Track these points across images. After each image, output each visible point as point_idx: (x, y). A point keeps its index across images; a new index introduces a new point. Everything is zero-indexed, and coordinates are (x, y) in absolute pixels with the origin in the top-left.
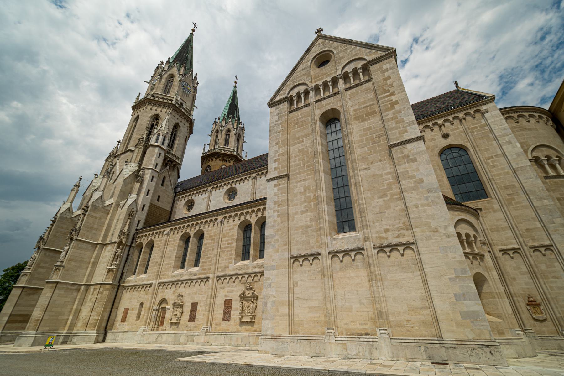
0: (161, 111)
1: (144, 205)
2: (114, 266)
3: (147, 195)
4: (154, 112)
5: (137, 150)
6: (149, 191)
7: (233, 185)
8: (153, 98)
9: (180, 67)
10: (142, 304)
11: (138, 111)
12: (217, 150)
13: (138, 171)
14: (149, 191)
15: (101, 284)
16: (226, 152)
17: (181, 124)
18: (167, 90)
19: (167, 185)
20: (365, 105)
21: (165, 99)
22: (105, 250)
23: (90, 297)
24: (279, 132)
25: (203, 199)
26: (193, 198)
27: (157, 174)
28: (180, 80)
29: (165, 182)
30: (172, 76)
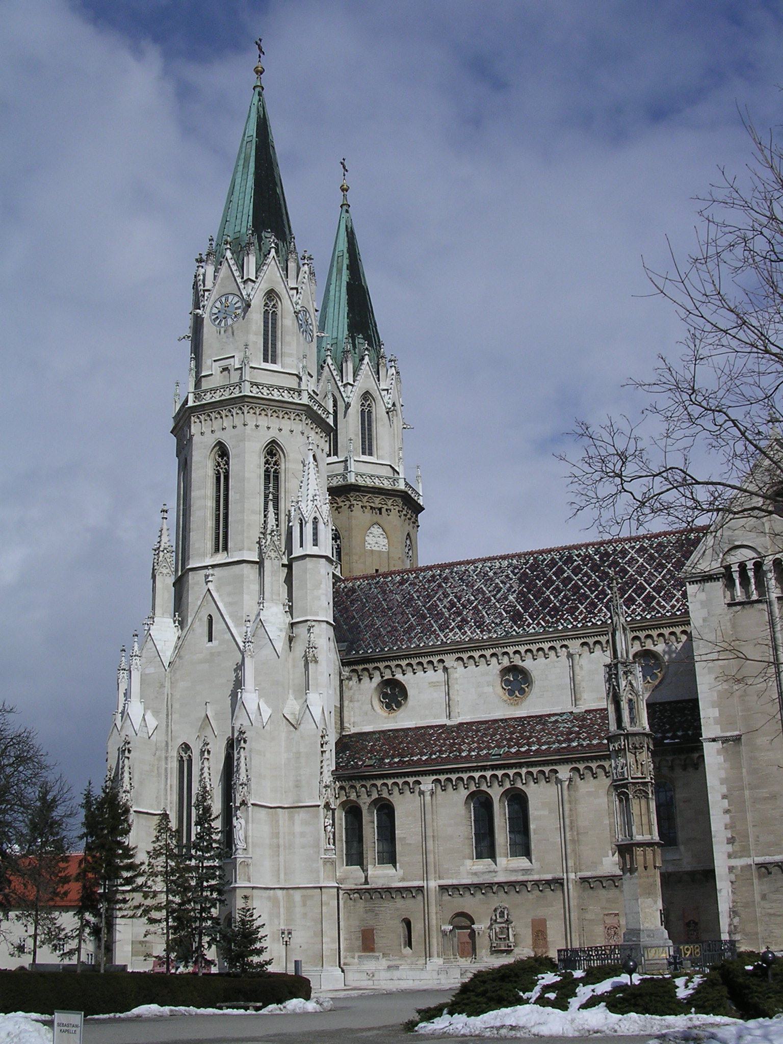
2: (330, 853)
7: (517, 661)
8: (255, 392)
9: (277, 252)
10: (408, 923)
11: (217, 424)
12: (352, 479)
13: (292, 625)
15: (321, 888)
16: (377, 483)
18: (270, 354)
21: (279, 388)
22: (291, 818)
23: (299, 910)
25: (433, 685)
26: (399, 676)
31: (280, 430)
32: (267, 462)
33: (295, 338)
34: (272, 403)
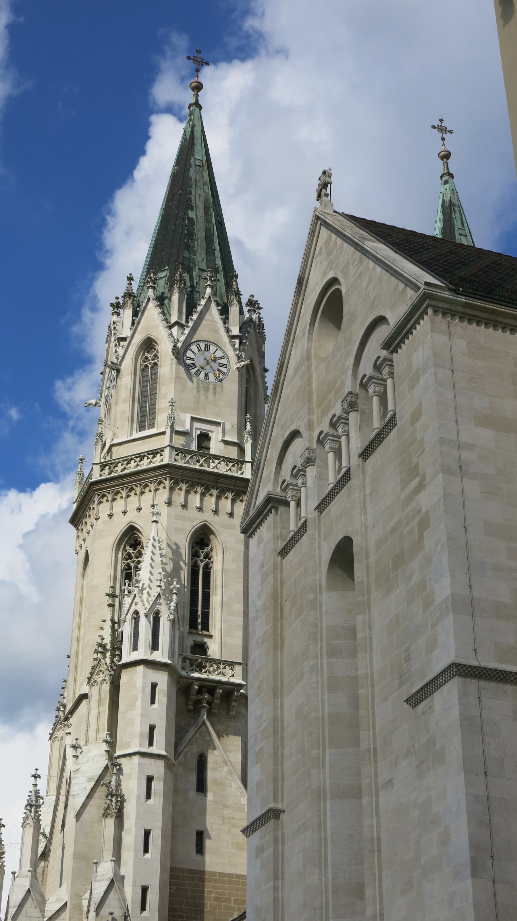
0: (139, 509)
1: (145, 890)
3: (146, 850)
4: (120, 525)
5: (96, 689)
6: (147, 833)
14: (147, 833)
17: (216, 523)
18: (145, 416)
19: (215, 781)
20: (391, 524)
21: (140, 456)
24: (263, 643)
27: (161, 764)
28: (179, 353)
29: (211, 775)
30: (149, 344)
31: (139, 509)
32: (129, 556)
33: (173, 386)
34: (125, 480)
